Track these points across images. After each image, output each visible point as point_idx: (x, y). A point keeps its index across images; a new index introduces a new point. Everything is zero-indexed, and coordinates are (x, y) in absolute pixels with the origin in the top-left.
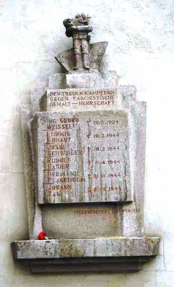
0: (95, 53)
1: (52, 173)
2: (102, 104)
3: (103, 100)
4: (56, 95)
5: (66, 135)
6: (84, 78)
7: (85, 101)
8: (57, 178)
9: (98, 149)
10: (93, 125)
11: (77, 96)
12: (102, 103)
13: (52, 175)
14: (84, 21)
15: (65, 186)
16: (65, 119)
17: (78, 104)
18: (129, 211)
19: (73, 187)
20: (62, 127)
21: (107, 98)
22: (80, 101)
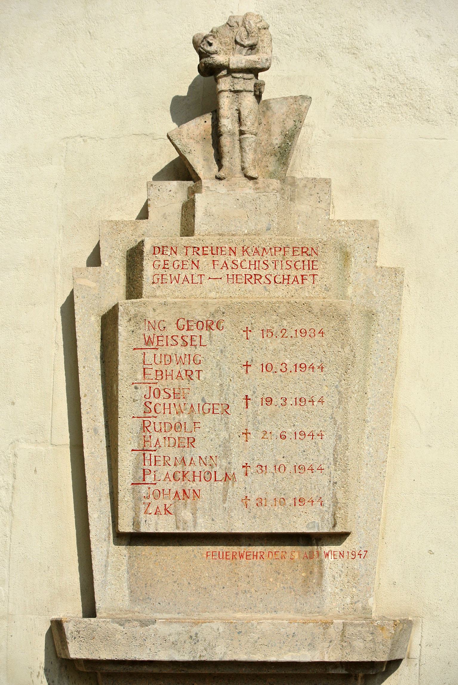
1: (153, 458)
2: (286, 281)
3: (289, 272)
4: (169, 253)
5: (192, 362)
6: (242, 206)
7: (243, 272)
8: (163, 470)
9: (269, 401)
10: (261, 339)
12: (286, 279)
13: (153, 464)
15: (184, 491)
16: (188, 321)
17: (225, 279)
20: (180, 342)
21: (299, 265)
22: (230, 272)
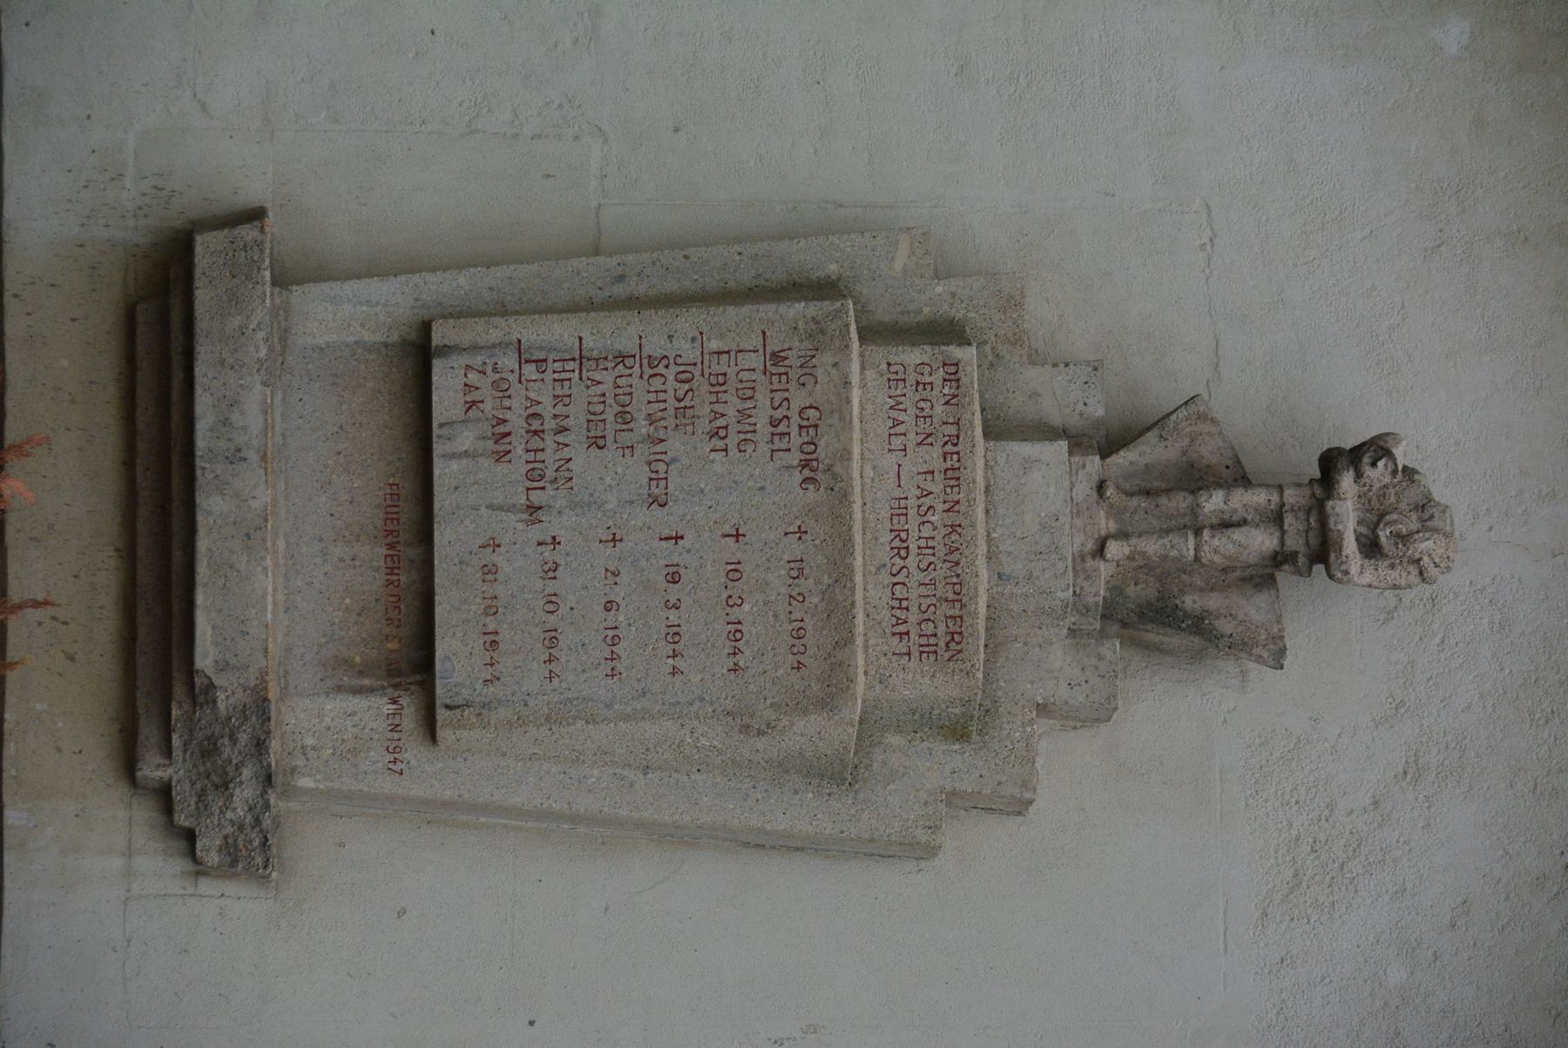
0: (1214, 602)
1: (567, 375)
2: (896, 604)
3: (914, 609)
4: (946, 391)
5: (742, 436)
6: (1044, 527)
7: (913, 525)
8: (545, 396)
9: (674, 579)
10: (786, 557)
11: (937, 488)
12: (901, 604)
13: (556, 376)
14: (1383, 539)
15: (508, 434)
16: (816, 426)
17: (898, 493)
18: (395, 728)
19: (502, 469)
20: (778, 414)
21: (929, 628)
22: (912, 502)
